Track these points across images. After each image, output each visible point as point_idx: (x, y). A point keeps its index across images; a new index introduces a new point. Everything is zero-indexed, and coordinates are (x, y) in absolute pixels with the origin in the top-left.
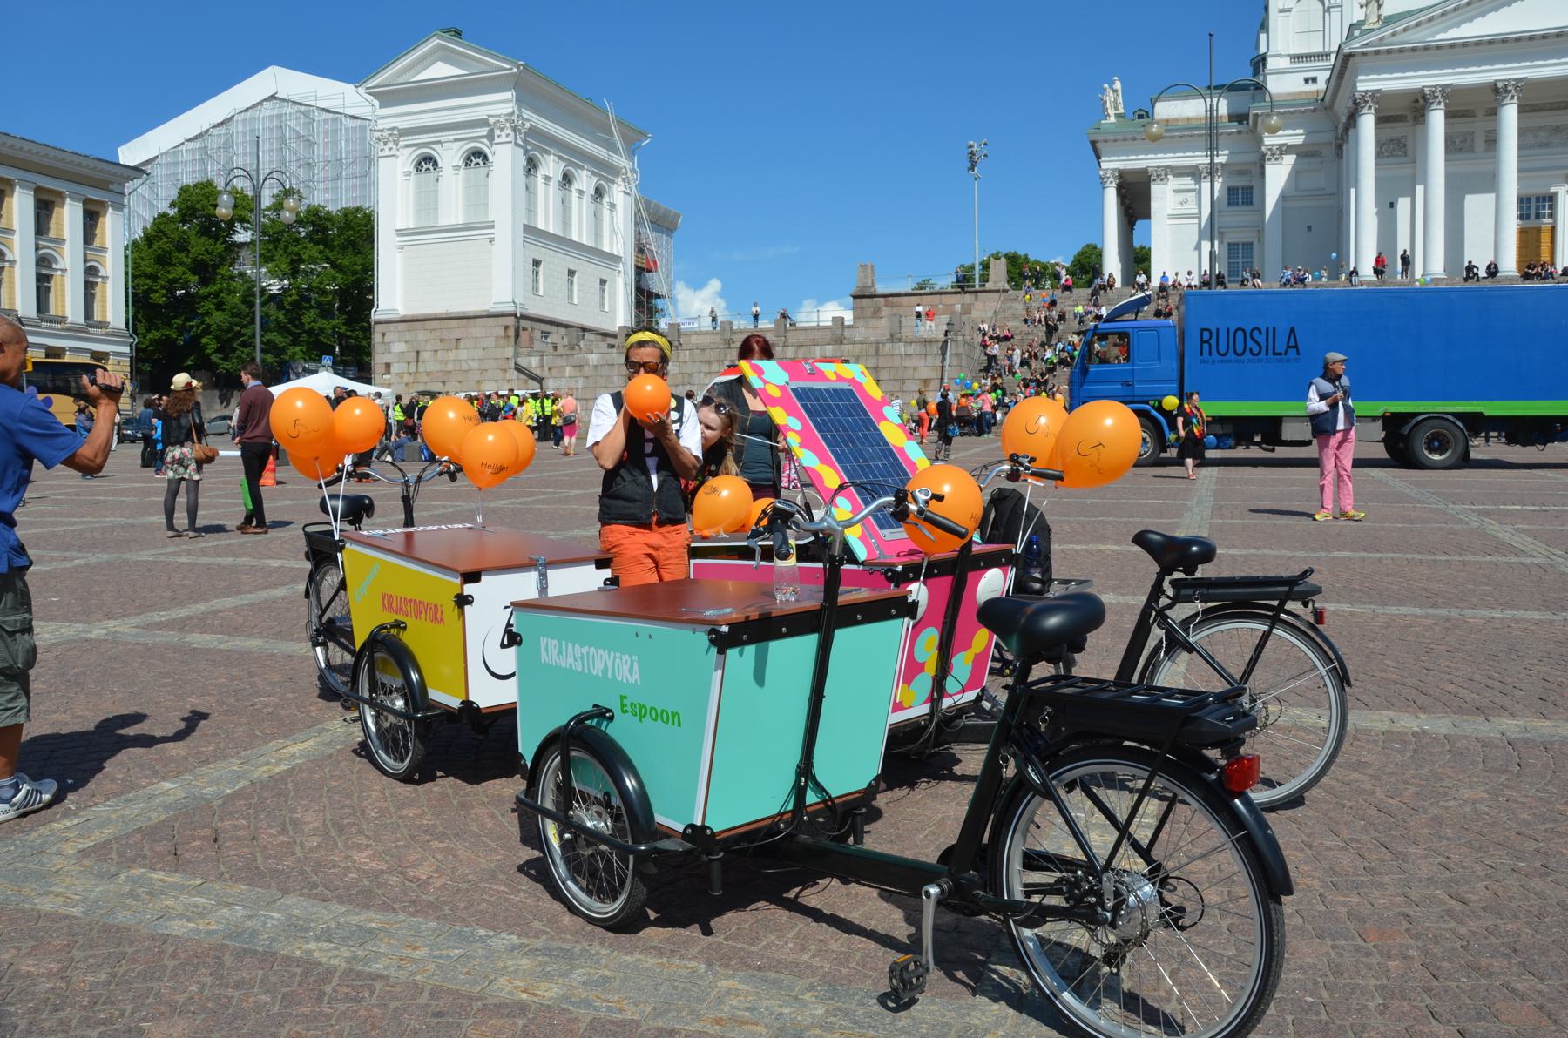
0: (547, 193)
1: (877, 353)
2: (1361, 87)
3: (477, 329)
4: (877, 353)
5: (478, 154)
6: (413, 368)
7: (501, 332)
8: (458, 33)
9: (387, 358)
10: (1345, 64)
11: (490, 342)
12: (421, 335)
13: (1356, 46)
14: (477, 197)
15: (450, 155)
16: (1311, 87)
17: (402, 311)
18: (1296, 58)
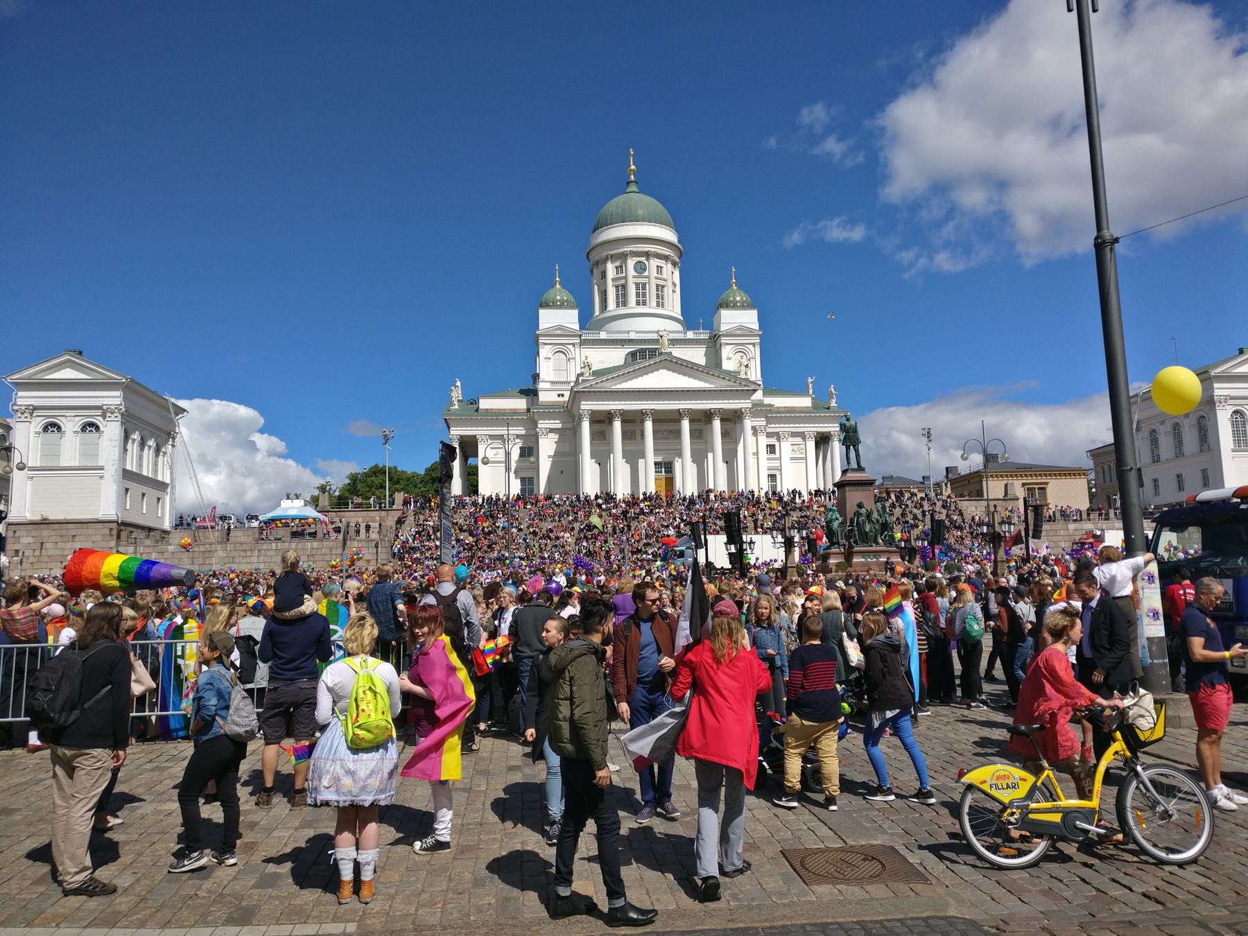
0: (133, 448)
3: (90, 530)
6: (37, 553)
8: (80, 353)
9: (16, 547)
10: (576, 395)
11: (99, 538)
12: (45, 533)
13: (580, 388)
14: (90, 451)
15: (71, 425)
16: (561, 399)
17: (29, 516)
18: (552, 382)
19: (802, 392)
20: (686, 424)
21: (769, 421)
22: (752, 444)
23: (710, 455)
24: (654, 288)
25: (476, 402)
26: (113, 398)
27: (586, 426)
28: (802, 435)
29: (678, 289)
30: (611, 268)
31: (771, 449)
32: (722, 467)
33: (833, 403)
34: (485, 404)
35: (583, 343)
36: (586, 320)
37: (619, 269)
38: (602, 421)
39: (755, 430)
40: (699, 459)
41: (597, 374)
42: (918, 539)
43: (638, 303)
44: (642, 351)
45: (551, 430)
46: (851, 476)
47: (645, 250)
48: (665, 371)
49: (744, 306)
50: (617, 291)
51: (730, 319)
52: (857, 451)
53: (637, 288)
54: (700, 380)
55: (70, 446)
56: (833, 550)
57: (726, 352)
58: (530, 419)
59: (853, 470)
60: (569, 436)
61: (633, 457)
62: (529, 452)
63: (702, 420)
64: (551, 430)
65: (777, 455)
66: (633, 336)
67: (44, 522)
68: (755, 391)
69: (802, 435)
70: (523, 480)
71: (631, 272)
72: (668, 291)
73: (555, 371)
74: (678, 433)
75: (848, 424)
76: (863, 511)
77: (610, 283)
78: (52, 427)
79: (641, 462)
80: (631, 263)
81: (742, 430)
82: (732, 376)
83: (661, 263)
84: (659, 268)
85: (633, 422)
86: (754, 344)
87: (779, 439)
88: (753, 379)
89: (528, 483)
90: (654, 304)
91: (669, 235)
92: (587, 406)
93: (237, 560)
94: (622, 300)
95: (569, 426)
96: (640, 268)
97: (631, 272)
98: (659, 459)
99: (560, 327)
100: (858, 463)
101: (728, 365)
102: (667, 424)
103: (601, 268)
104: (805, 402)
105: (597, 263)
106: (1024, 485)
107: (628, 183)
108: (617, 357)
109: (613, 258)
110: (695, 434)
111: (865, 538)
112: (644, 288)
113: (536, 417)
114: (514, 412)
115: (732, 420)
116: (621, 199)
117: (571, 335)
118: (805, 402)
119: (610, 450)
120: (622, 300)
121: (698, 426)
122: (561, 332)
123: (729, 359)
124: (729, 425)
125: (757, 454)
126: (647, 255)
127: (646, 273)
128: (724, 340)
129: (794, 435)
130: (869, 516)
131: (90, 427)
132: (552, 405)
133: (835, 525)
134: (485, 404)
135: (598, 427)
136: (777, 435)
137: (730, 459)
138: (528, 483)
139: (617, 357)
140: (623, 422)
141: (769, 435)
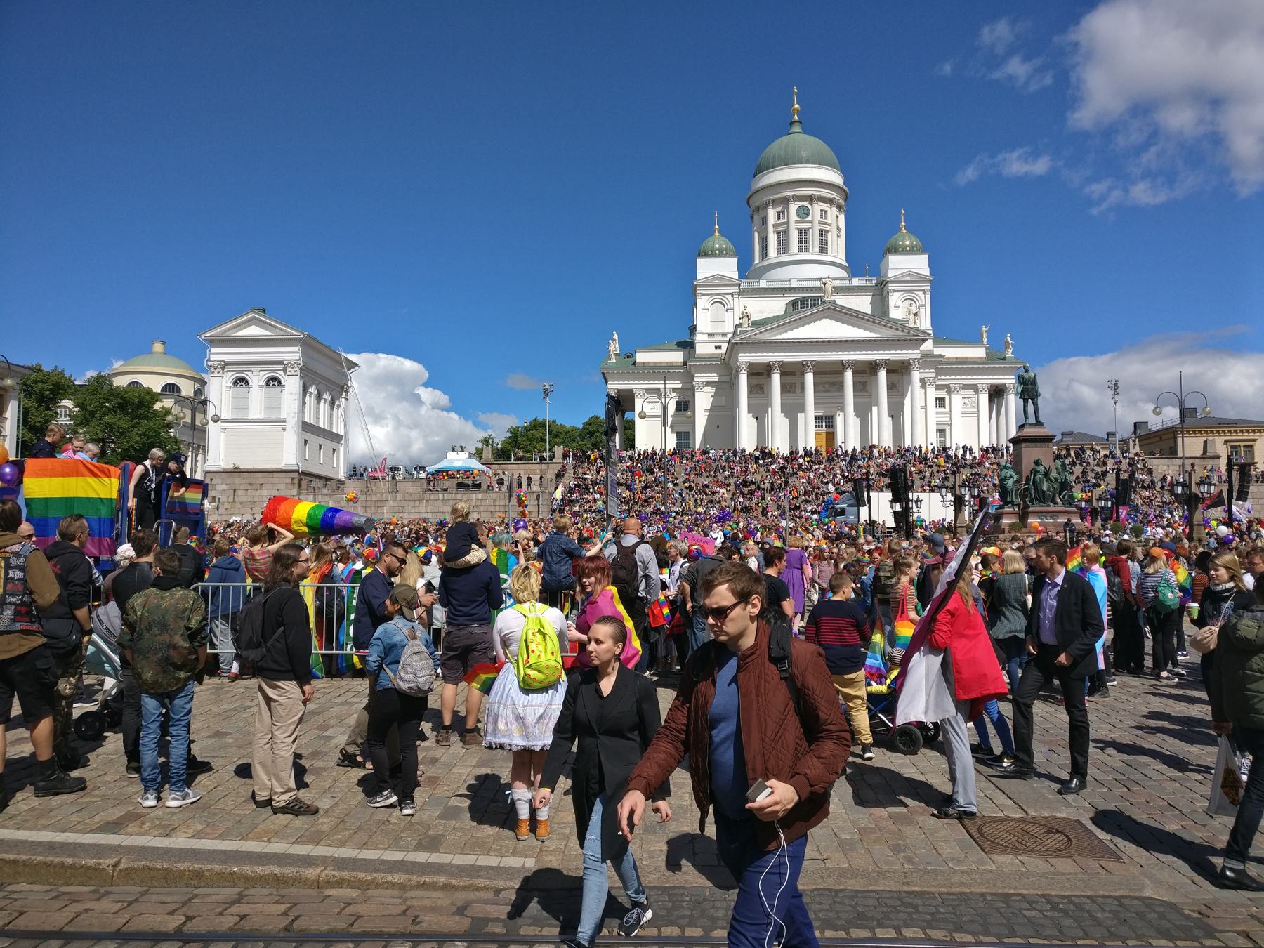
0: (311, 401)
3: (275, 479)
5: (274, 379)
6: (231, 499)
7: (289, 481)
8: (264, 311)
10: (734, 347)
11: (282, 486)
12: (237, 481)
13: (738, 339)
14: (273, 404)
15: (257, 379)
16: (718, 351)
17: (224, 465)
18: (709, 334)
19: (976, 342)
20: (849, 376)
21: (939, 372)
22: (919, 397)
23: (875, 409)
24: (817, 233)
25: (633, 356)
26: (292, 354)
27: (743, 379)
28: (975, 388)
29: (843, 234)
30: (772, 214)
31: (941, 402)
32: (887, 422)
33: (1009, 354)
34: (642, 357)
35: (742, 292)
36: (745, 269)
37: (781, 214)
38: (760, 374)
39: (923, 383)
40: (863, 413)
41: (756, 324)
42: (1100, 499)
43: (800, 250)
44: (804, 300)
45: (708, 384)
46: (1028, 431)
47: (808, 193)
49: (913, 251)
50: (778, 237)
51: (897, 264)
52: (1035, 405)
53: (800, 234)
54: (865, 329)
55: (257, 400)
56: (1007, 510)
57: (894, 299)
58: (686, 373)
59: (1031, 425)
60: (726, 389)
61: (792, 410)
62: (685, 405)
63: (867, 371)
64: (708, 384)
65: (947, 409)
66: (794, 284)
67: (236, 471)
68: (924, 340)
69: (975, 388)
70: (679, 435)
71: (794, 217)
72: (832, 236)
73: (713, 322)
74: (840, 386)
75: (1026, 375)
76: (1041, 469)
77: (771, 229)
78: (241, 381)
79: (801, 416)
80: (793, 207)
81: (910, 383)
82: (900, 325)
83: (825, 206)
84: (823, 212)
85: (792, 374)
86: (924, 291)
87: (949, 392)
88: (922, 328)
89: (684, 438)
90: (817, 250)
91: (835, 177)
92: (745, 358)
93: (406, 509)
94: (784, 247)
95: (727, 378)
96: (803, 213)
97: (794, 217)
98: (820, 413)
99: (718, 277)
100: (1037, 418)
101: (896, 313)
102: (829, 376)
103: (762, 214)
104: (979, 352)
105: (758, 209)
106: (1226, 442)
107: (791, 124)
108: (775, 306)
109: (774, 203)
110: (858, 387)
111: (1042, 497)
112: (807, 234)
113: (693, 370)
114: (670, 366)
115: (899, 371)
116: (785, 139)
117: (730, 284)
118: (979, 352)
119: (769, 404)
120: (784, 247)
121: (861, 378)
122: (719, 282)
123: (897, 306)
124: (895, 377)
125: (925, 407)
126: (811, 199)
127: (809, 218)
128: (891, 287)
129: (966, 387)
130: (1047, 474)
131: (273, 381)
132: (710, 358)
133: (1010, 483)
134: (642, 357)
135: (756, 380)
136: (948, 388)
137: (896, 413)
138: (684, 438)
139: (775, 306)
140: (782, 374)
141: (939, 388)
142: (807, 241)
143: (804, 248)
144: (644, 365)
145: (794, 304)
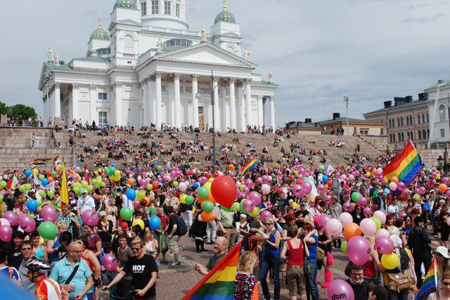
1: (45, 152)
2: (158, 70)
4: (45, 152)
13: (157, 58)
16: (129, 64)
20: (215, 84)
27: (159, 81)
28: (256, 96)
44: (179, 40)
48: (206, 52)
61: (186, 102)
63: (224, 82)
66: (167, 31)
69: (256, 96)
85: (186, 81)
86: (238, 43)
92: (161, 69)
102: (205, 83)
114: (96, 71)
132: (125, 68)
142: (169, 8)
143: (167, 11)
144: (79, 69)
145: (171, 42)
